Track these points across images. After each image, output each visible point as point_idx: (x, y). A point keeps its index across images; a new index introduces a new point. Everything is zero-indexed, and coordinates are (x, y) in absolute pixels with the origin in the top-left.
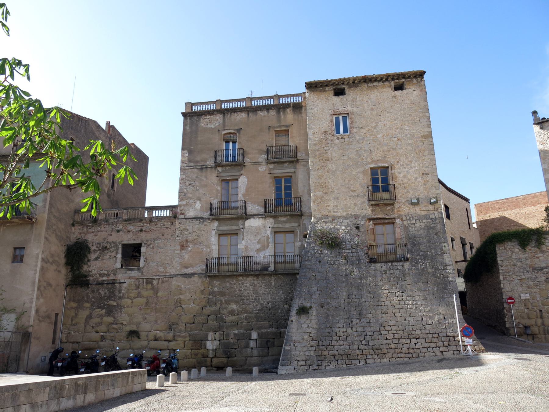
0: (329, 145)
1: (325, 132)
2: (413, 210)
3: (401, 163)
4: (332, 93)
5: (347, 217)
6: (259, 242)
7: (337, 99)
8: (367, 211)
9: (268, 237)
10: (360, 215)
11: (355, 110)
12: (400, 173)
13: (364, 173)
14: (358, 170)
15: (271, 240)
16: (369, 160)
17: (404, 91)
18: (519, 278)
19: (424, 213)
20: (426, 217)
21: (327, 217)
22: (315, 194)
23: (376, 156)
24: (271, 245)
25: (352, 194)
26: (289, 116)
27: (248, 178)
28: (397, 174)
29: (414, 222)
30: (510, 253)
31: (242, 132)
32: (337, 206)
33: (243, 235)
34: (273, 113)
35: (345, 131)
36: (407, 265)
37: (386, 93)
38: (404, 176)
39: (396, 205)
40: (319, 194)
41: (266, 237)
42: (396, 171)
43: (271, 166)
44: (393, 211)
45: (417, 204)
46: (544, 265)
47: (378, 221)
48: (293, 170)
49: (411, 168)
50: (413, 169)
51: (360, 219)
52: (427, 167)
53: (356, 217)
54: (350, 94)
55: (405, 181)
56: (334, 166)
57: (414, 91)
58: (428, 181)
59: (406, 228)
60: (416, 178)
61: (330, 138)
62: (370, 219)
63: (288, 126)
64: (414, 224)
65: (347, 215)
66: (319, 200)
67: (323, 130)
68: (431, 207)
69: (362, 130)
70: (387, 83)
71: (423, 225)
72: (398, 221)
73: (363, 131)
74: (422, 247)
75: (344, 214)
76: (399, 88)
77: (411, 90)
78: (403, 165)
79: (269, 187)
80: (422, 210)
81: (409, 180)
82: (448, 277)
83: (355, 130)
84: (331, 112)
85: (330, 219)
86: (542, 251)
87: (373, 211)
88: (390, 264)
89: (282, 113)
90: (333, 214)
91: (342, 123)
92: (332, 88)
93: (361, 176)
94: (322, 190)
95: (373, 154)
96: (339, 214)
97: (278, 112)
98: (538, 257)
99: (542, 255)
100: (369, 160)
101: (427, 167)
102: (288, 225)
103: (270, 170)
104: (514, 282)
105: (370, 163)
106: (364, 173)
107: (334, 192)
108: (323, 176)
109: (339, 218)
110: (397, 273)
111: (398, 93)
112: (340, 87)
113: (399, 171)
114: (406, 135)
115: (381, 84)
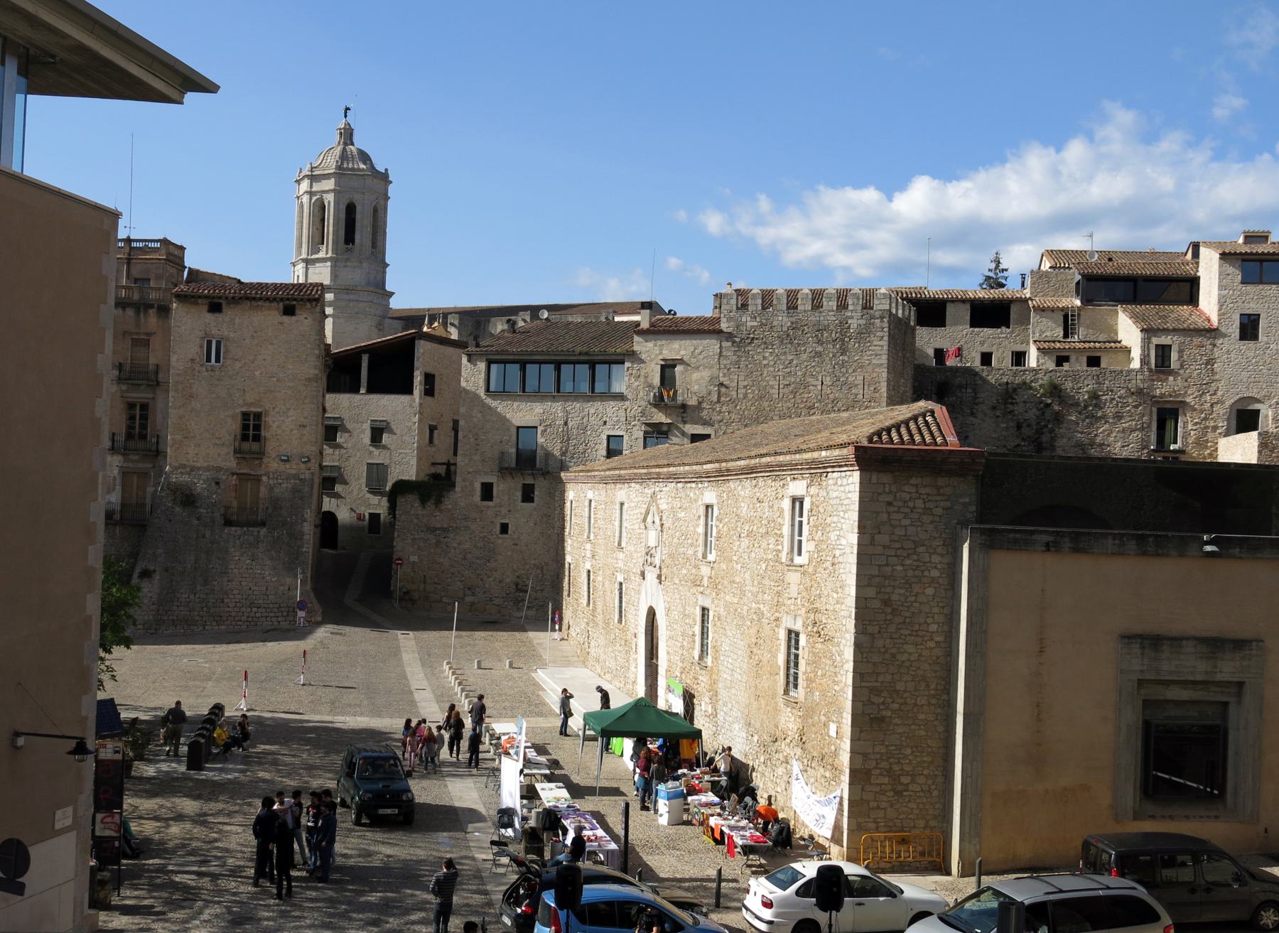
2: (282, 467)
4: (206, 307)
5: (207, 469)
7: (210, 317)
8: (232, 463)
11: (232, 335)
15: (118, 481)
16: (241, 402)
17: (294, 318)
19: (293, 472)
20: (296, 476)
21: (184, 466)
23: (250, 398)
24: (118, 488)
26: (152, 320)
34: (130, 312)
35: (218, 360)
36: (263, 531)
37: (270, 318)
38: (278, 427)
39: (265, 460)
40: (178, 437)
42: (269, 419)
43: (124, 388)
44: (260, 465)
45: (288, 461)
46: (438, 526)
47: (243, 477)
48: (151, 396)
53: (219, 469)
54: (229, 313)
55: (279, 432)
59: (271, 489)
62: (233, 474)
63: (149, 334)
68: (303, 466)
70: (275, 304)
72: (264, 479)
73: (238, 365)
76: (289, 311)
77: (302, 317)
80: (292, 468)
83: (229, 362)
84: (201, 334)
86: (440, 511)
91: (214, 350)
92: (206, 301)
93: (230, 420)
97: (138, 312)
100: (241, 402)
102: (140, 465)
103: (123, 391)
109: (199, 469)
110: (251, 539)
111: (286, 319)
112: (217, 301)
115: (267, 304)
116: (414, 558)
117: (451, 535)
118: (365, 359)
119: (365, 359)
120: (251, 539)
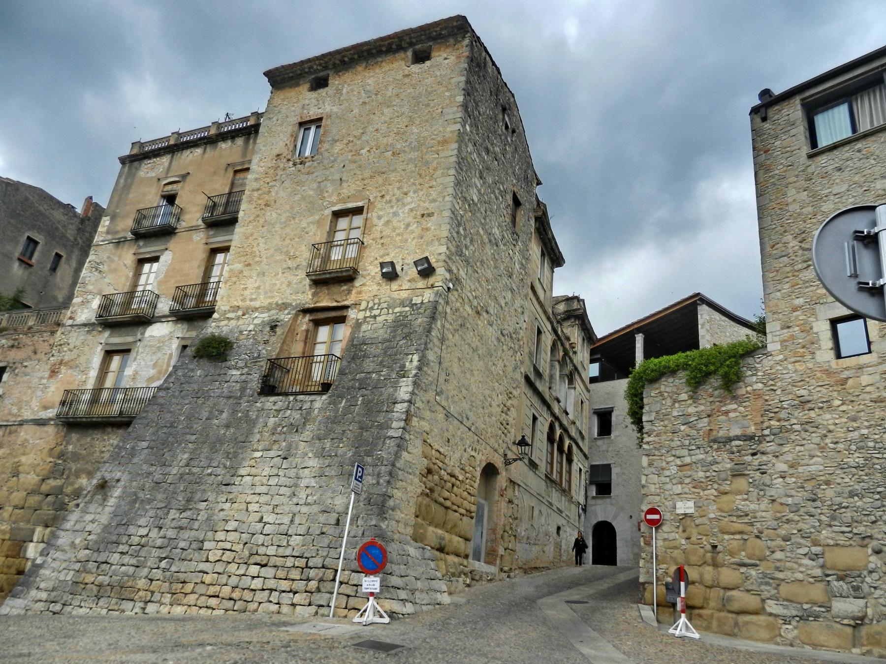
0: (278, 177)
1: (278, 155)
3: (387, 198)
6: (155, 365)
9: (171, 355)
10: (291, 305)
12: (379, 218)
13: (319, 223)
14: (311, 219)
16: (334, 198)
17: (428, 63)
18: (678, 462)
22: (232, 267)
25: (290, 263)
27: (174, 253)
28: (375, 220)
29: (376, 312)
30: (669, 402)
31: (188, 179)
32: (258, 288)
33: (137, 352)
37: (396, 70)
41: (167, 356)
46: (736, 431)
49: (404, 205)
50: (408, 207)
51: (286, 312)
52: (434, 201)
53: (283, 306)
55: (387, 231)
56: (274, 215)
57: (446, 59)
58: (428, 229)
60: (408, 225)
61: (282, 166)
62: (306, 311)
64: (375, 317)
65: (270, 304)
66: (234, 279)
67: (276, 152)
69: (338, 144)
71: (390, 318)
73: (337, 148)
74: (369, 365)
75: (266, 303)
76: (421, 57)
78: (390, 201)
79: (199, 267)
81: (394, 229)
82: (389, 427)
85: (240, 313)
86: (735, 398)
87: (314, 295)
88: (291, 398)
89: (251, 141)
90: (248, 303)
94: (243, 259)
95: (345, 185)
96: (257, 304)
97: (247, 141)
98: (727, 413)
99: (735, 406)
100: (334, 198)
101: (434, 201)
104: (667, 473)
105: (334, 204)
106: (319, 223)
107: (261, 262)
108: (252, 235)
111: (416, 68)
113: (381, 213)
114: (411, 144)
116: (685, 507)
117: (770, 447)
118: (639, 339)
119: (639, 339)
120: (297, 415)
